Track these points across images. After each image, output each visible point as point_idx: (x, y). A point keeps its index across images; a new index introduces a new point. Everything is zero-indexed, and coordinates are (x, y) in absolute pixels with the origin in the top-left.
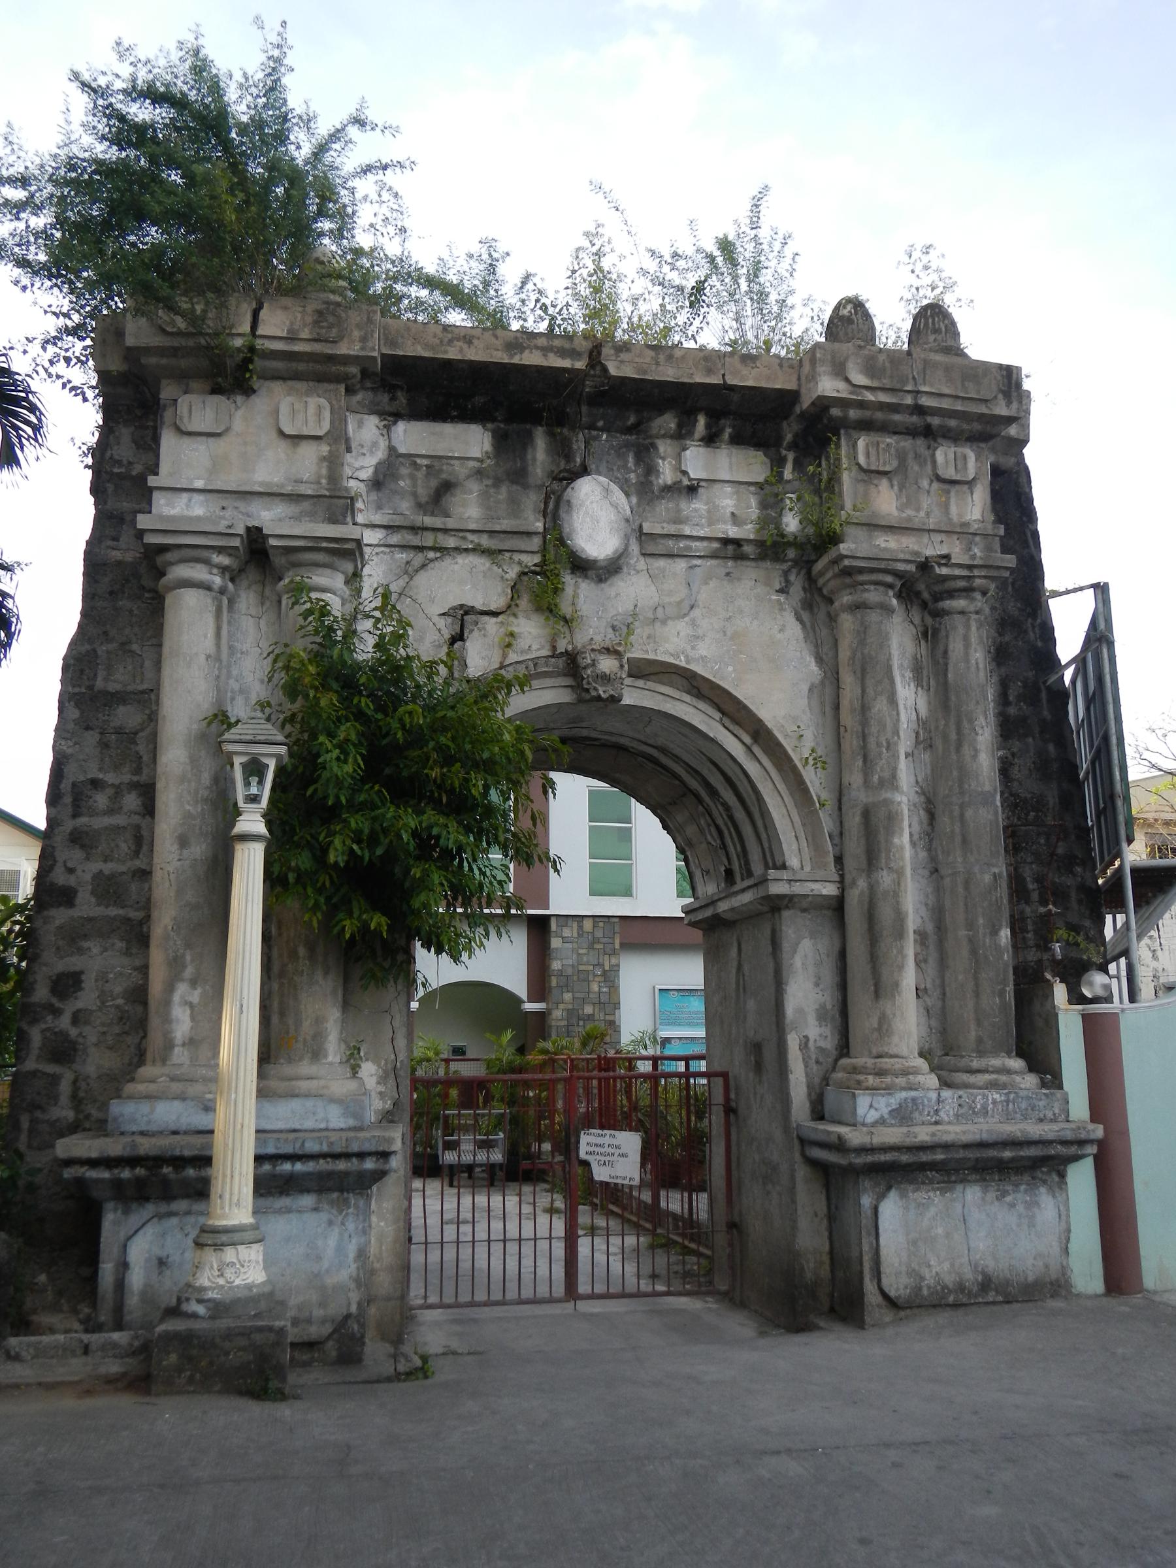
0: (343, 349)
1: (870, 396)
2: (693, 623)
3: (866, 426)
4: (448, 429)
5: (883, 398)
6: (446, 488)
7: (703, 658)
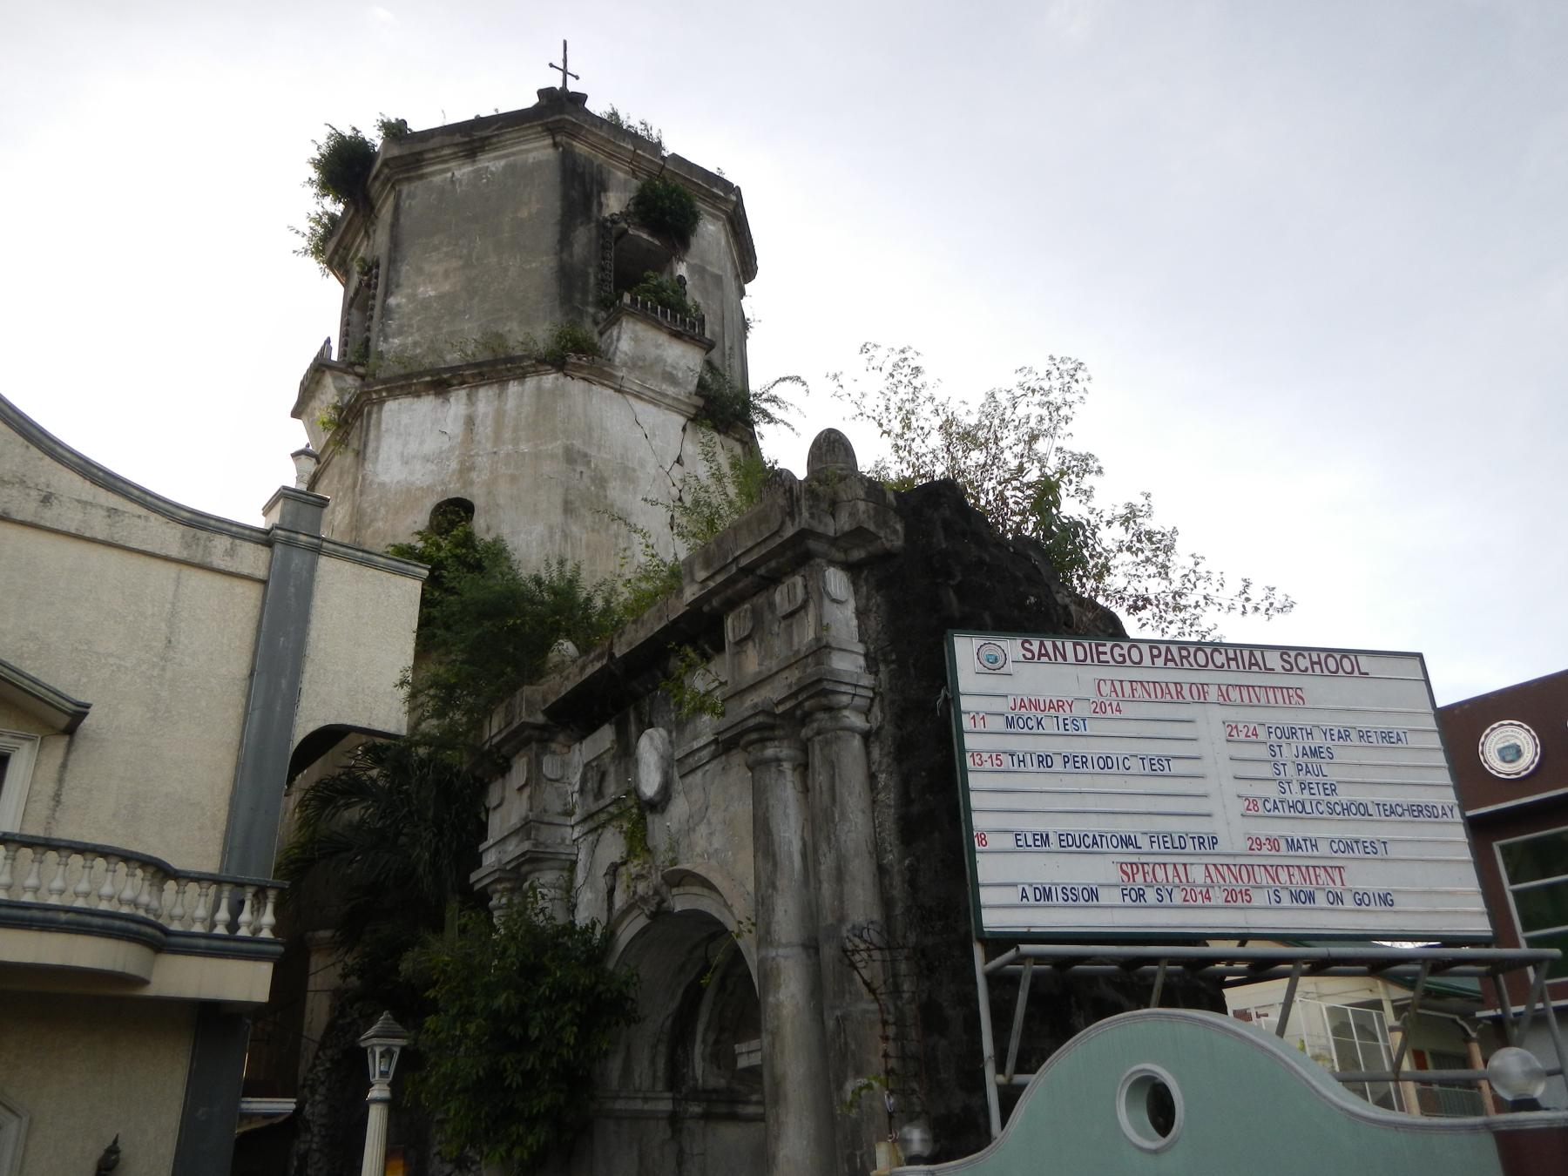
0: (515, 724)
1: (712, 584)
2: (709, 823)
3: (731, 604)
4: (597, 735)
5: (720, 579)
6: (603, 775)
7: (716, 850)
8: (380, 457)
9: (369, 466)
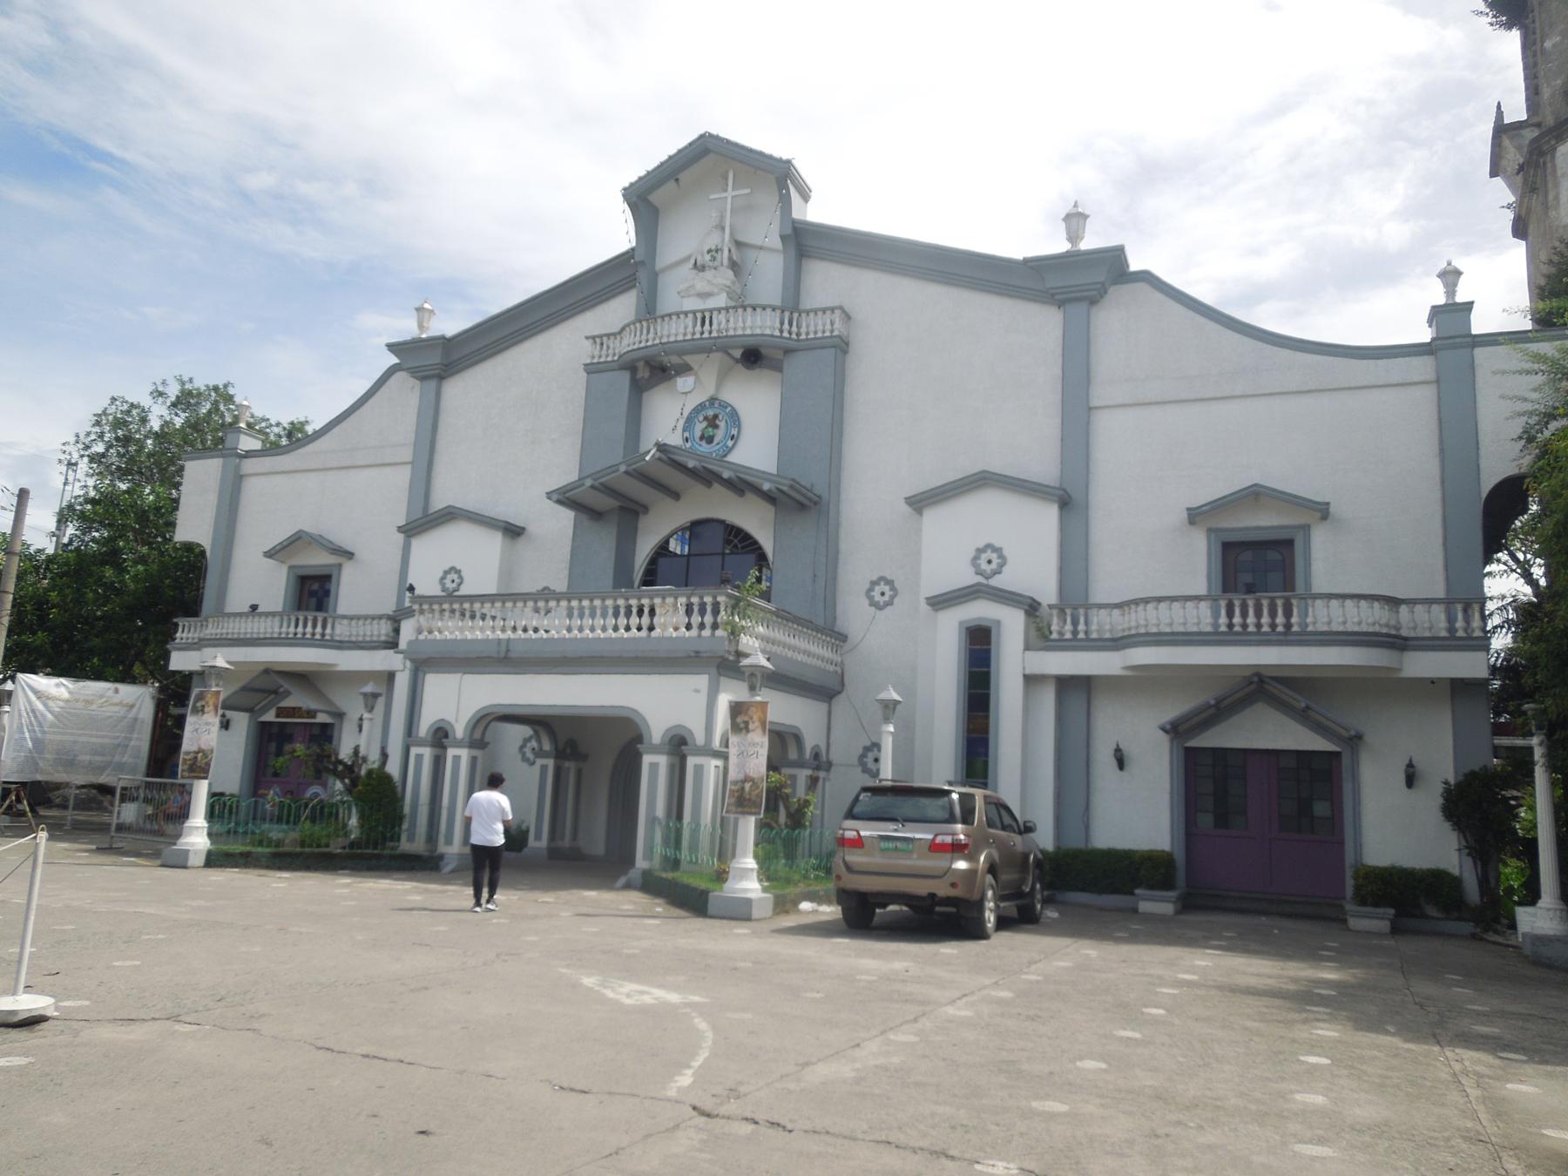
8: (1561, 202)
9: (1552, 214)
